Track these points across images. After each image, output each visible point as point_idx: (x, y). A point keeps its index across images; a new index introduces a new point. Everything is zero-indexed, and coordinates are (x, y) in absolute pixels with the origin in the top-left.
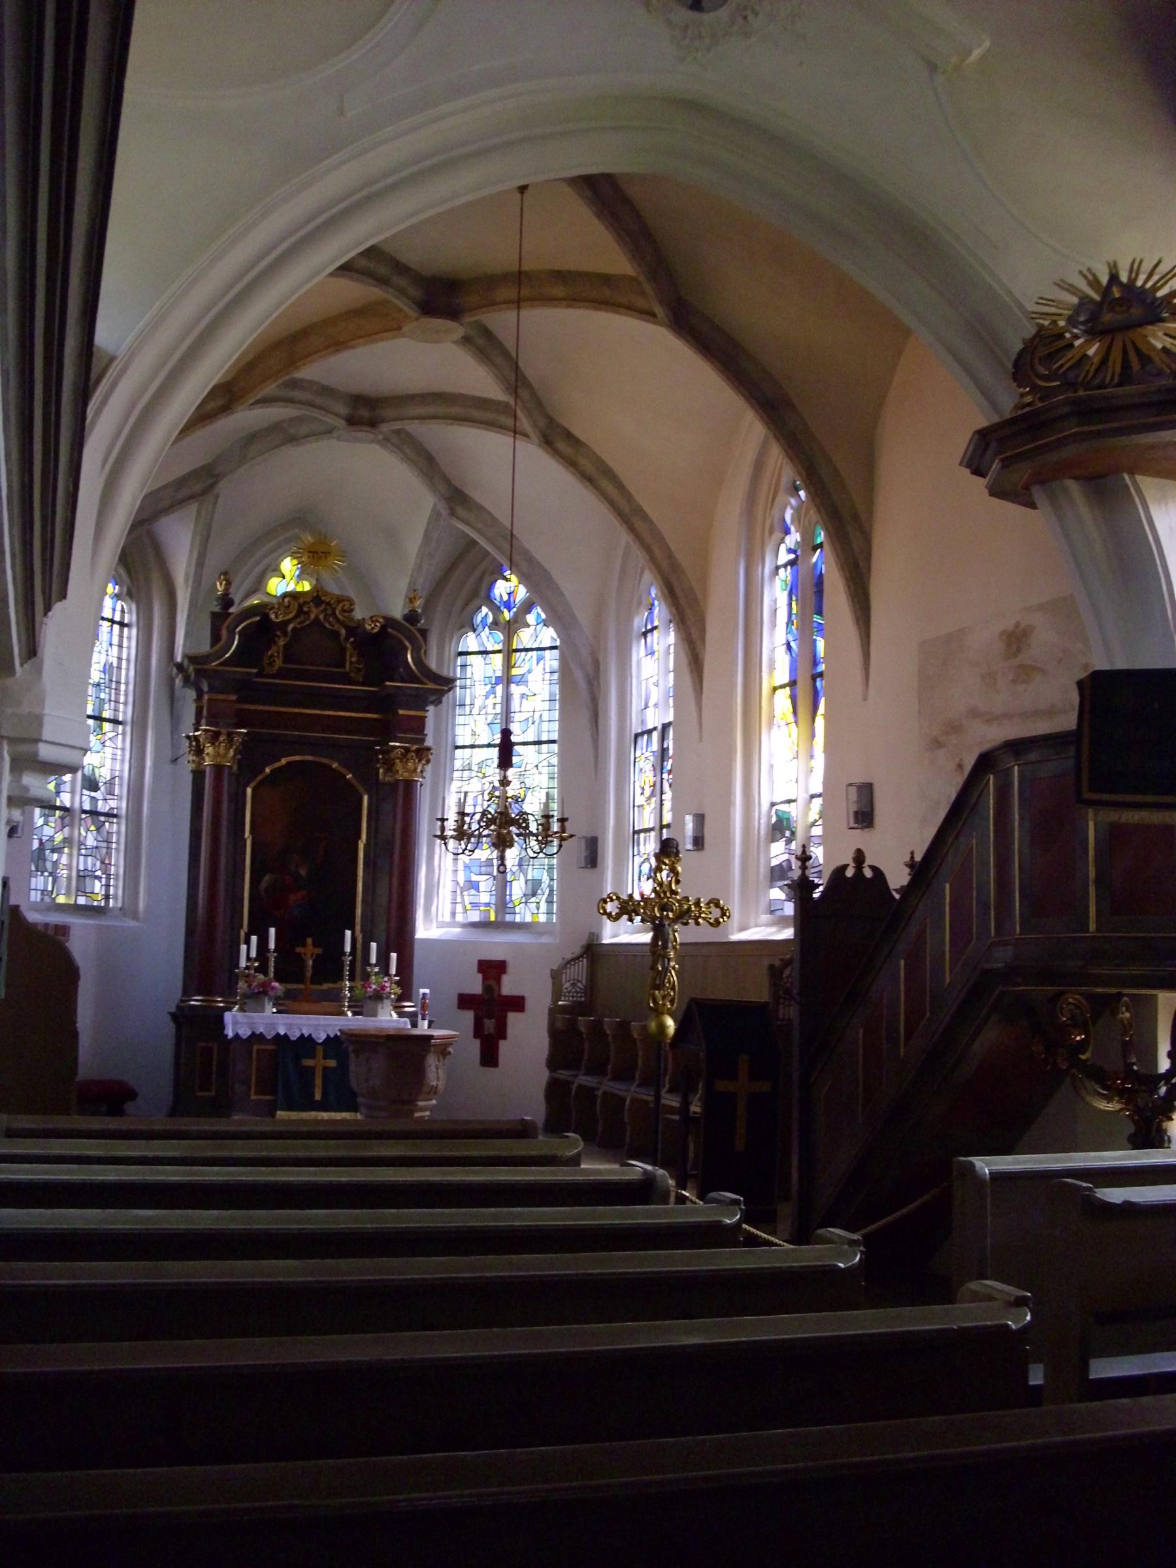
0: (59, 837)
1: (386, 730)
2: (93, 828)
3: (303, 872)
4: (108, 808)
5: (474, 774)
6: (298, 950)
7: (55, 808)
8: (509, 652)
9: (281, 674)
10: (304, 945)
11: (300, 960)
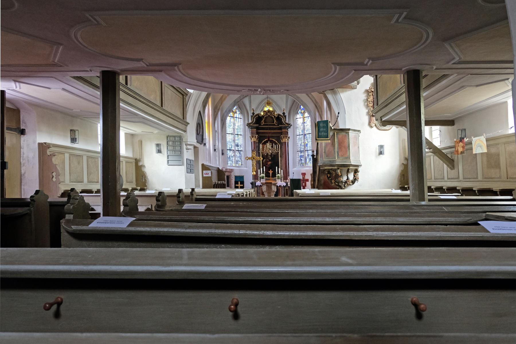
1: (281, 133)
9: (264, 125)
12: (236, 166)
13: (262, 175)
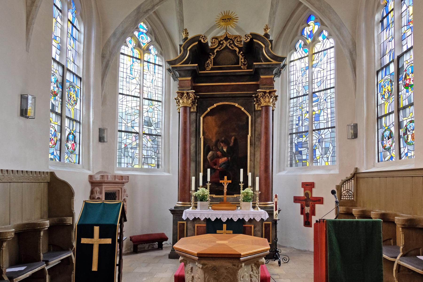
0: (134, 144)
2: (150, 140)
3: (225, 150)
4: (157, 132)
5: (298, 108)
6: (221, 181)
7: (132, 132)
8: (311, 56)
10: (223, 179)
11: (222, 185)
12: (141, 170)
13: (202, 191)
